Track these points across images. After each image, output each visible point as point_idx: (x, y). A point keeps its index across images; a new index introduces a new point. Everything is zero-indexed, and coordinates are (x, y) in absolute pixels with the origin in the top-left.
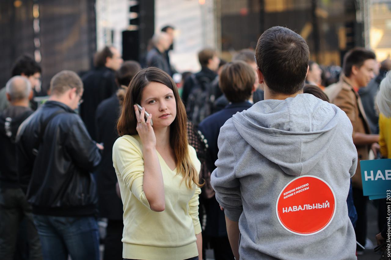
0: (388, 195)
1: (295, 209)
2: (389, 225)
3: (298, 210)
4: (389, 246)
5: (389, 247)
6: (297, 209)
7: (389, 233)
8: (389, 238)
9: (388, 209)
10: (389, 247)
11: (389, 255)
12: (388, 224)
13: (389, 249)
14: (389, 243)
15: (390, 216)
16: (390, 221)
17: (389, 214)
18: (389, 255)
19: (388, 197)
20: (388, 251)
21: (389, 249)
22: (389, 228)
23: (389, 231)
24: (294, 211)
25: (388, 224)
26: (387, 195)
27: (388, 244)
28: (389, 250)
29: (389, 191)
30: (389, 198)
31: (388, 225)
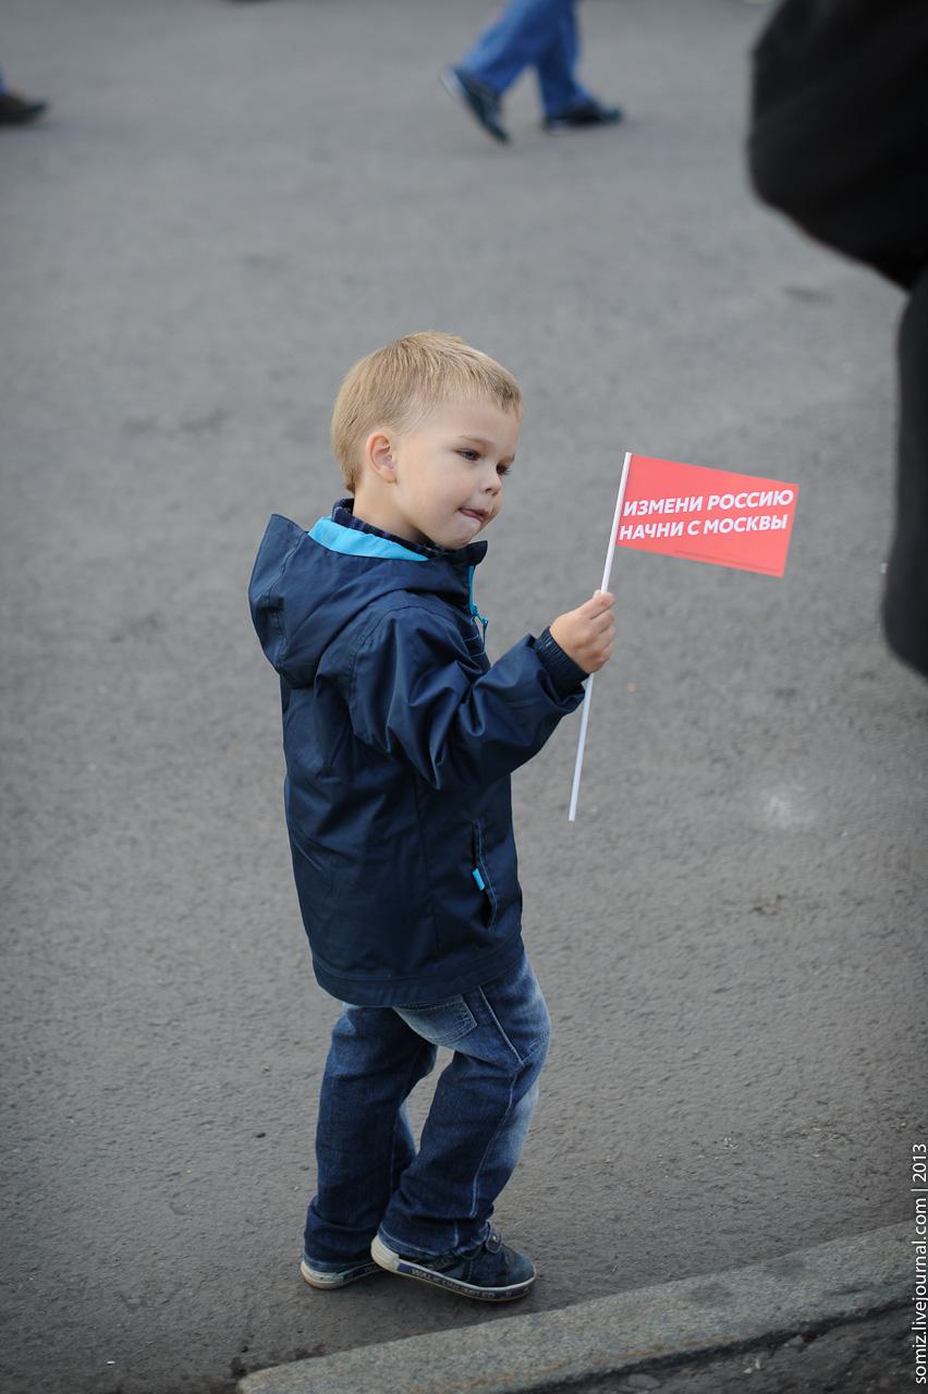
0: (918, 1161)
2: (921, 1267)
4: (920, 1343)
5: (922, 1348)
7: (923, 1296)
8: (920, 1316)
9: (918, 1212)
11: (920, 1377)
14: (920, 1333)
18: (920, 1377)
19: (917, 1168)
20: (918, 1362)
22: (922, 1280)
25: (918, 1264)
28: (920, 1359)
29: (922, 1148)
30: (922, 1174)
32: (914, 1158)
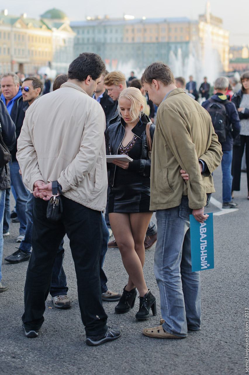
0: (246, 312)
4: (247, 361)
6: (202, 232)
11: (247, 371)
13: (247, 364)
14: (247, 359)
16: (247, 338)
18: (247, 371)
19: (246, 314)
20: (246, 366)
21: (247, 364)
22: (247, 344)
23: (247, 347)
24: (201, 229)
28: (247, 366)
30: (247, 316)
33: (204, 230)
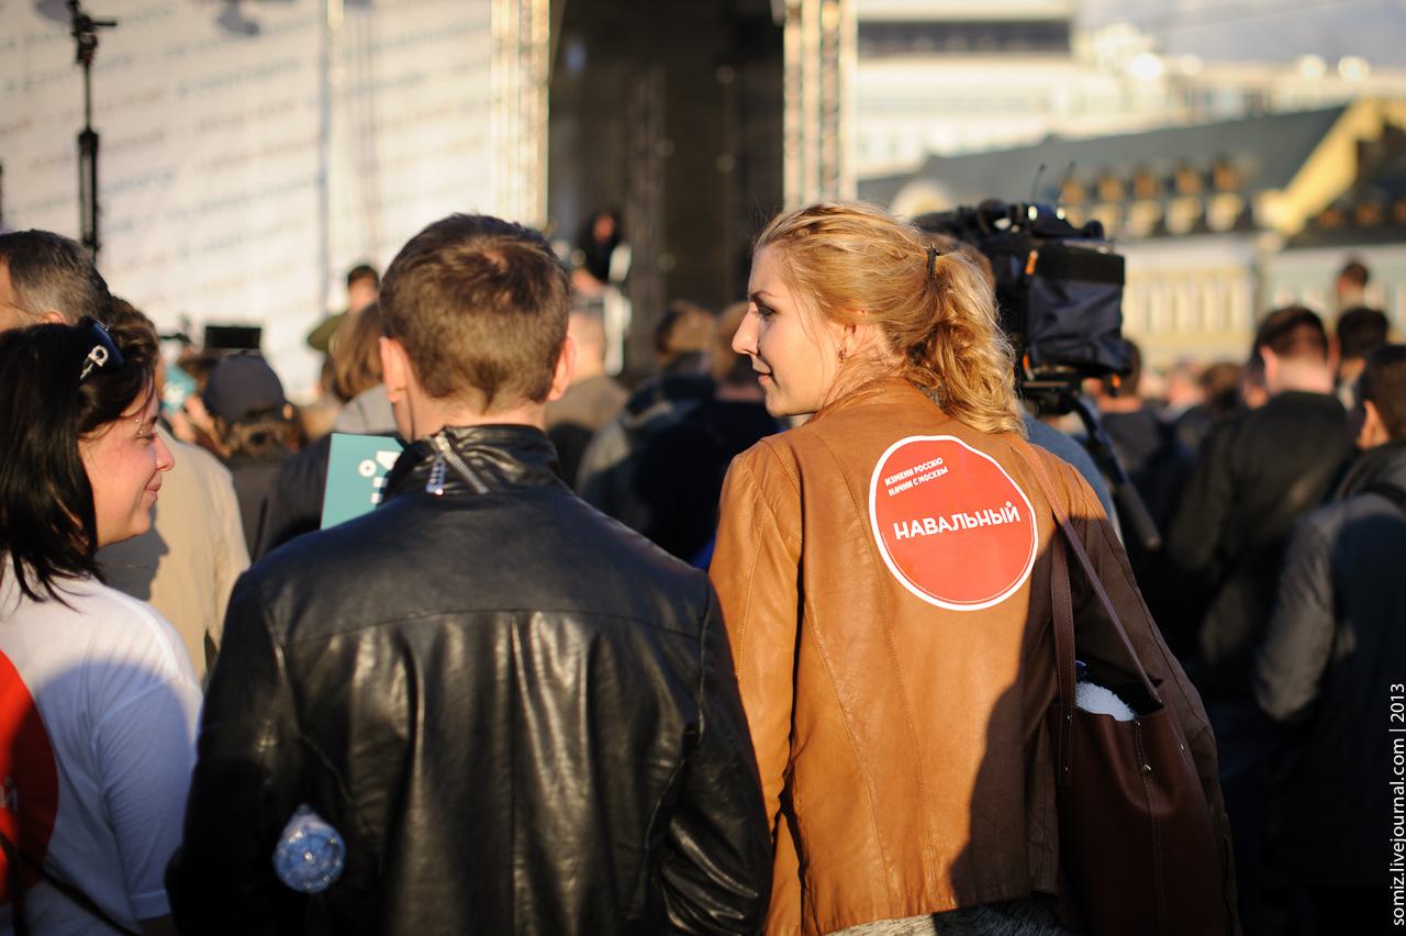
0: (1396, 701)
1: (931, 527)
2: (1399, 808)
3: (941, 531)
4: (1398, 884)
5: (1399, 890)
6: (935, 527)
8: (1398, 857)
9: (1396, 752)
10: (1399, 890)
11: (1398, 919)
12: (1396, 805)
13: (1398, 895)
14: (1398, 875)
15: (1401, 776)
17: (1399, 770)
18: (1398, 919)
19: (1394, 708)
20: (1396, 904)
21: (1398, 895)
22: (1400, 821)
23: (1399, 831)
25: (1396, 805)
26: (1393, 703)
27: (1395, 879)
28: (1398, 901)
29: (1400, 688)
30: (1400, 714)
31: (1396, 811)
32: (1392, 698)
33: (930, 523)
